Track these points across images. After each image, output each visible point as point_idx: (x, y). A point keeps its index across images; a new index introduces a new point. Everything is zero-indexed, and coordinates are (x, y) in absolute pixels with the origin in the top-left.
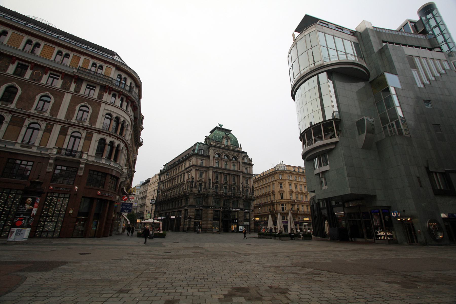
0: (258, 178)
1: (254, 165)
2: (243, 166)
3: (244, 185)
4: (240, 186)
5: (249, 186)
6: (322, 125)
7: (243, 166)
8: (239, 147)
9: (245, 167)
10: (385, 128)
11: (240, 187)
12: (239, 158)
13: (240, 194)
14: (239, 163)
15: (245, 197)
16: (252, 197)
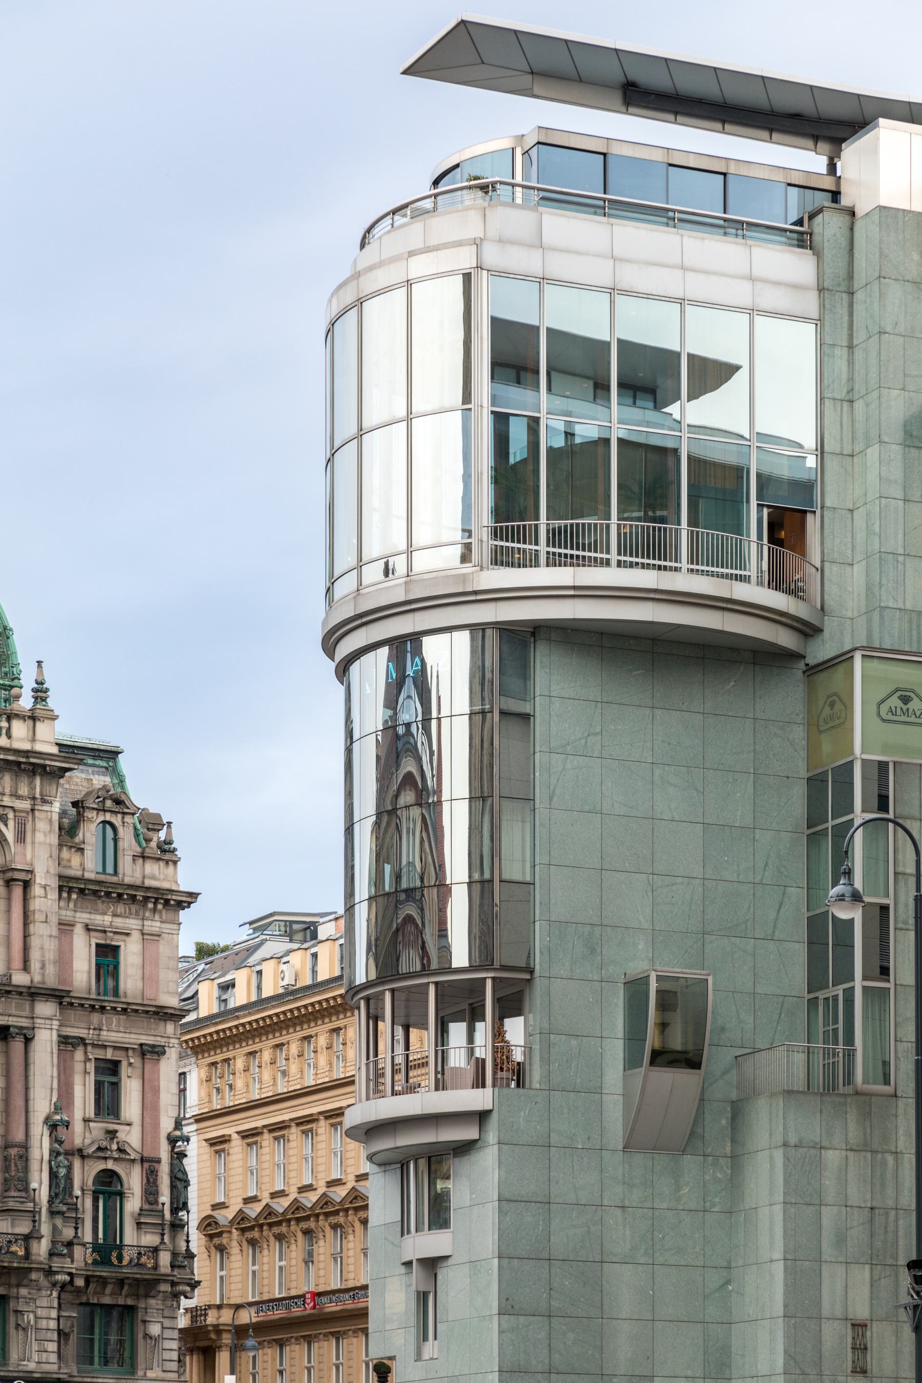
0: (290, 993)
1: (194, 896)
2: (65, 927)
3: (79, 1135)
4: (25, 1146)
5: (132, 1137)
6: (432, 990)
7: (65, 927)
8: (26, 702)
9: (88, 929)
10: (813, 1003)
11: (25, 1158)
12: (21, 837)
13: (24, 1228)
14: (18, 891)
15: (81, 1257)
16: (165, 1258)
